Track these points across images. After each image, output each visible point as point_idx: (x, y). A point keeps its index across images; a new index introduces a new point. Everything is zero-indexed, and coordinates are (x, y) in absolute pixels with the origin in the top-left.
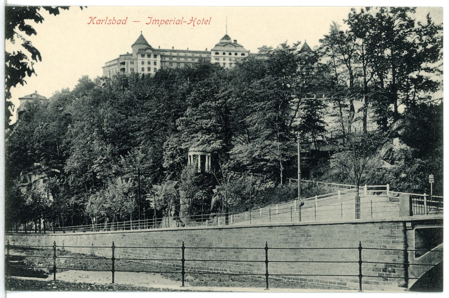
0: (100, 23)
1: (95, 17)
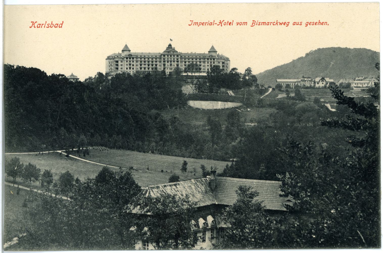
1: (36, 22)
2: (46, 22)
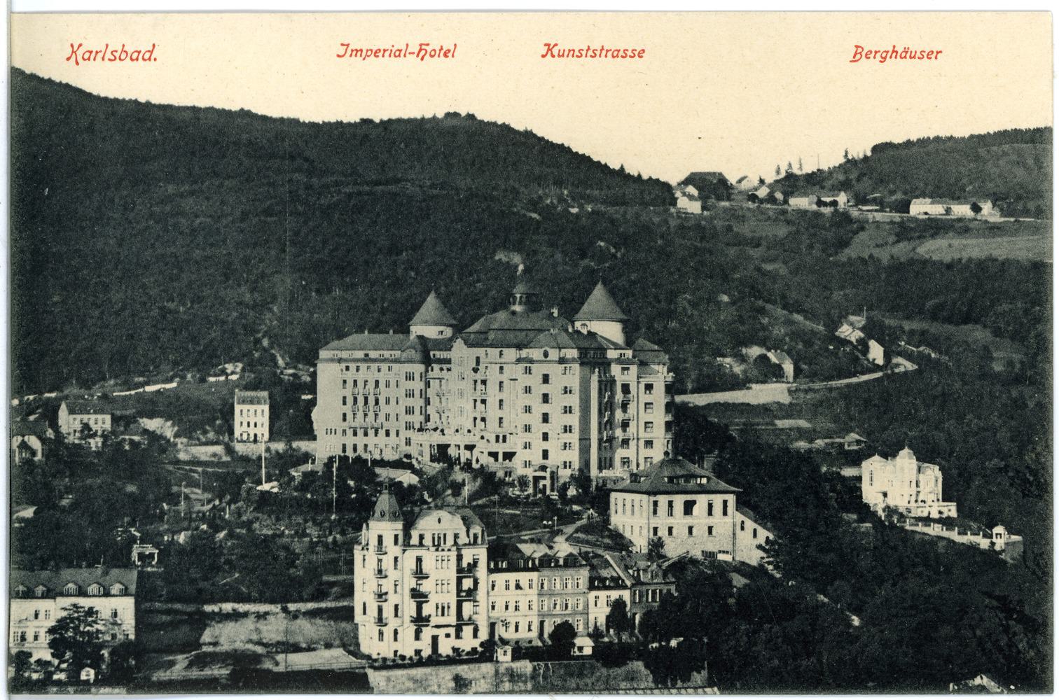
0: (92, 57)
2: (107, 46)
